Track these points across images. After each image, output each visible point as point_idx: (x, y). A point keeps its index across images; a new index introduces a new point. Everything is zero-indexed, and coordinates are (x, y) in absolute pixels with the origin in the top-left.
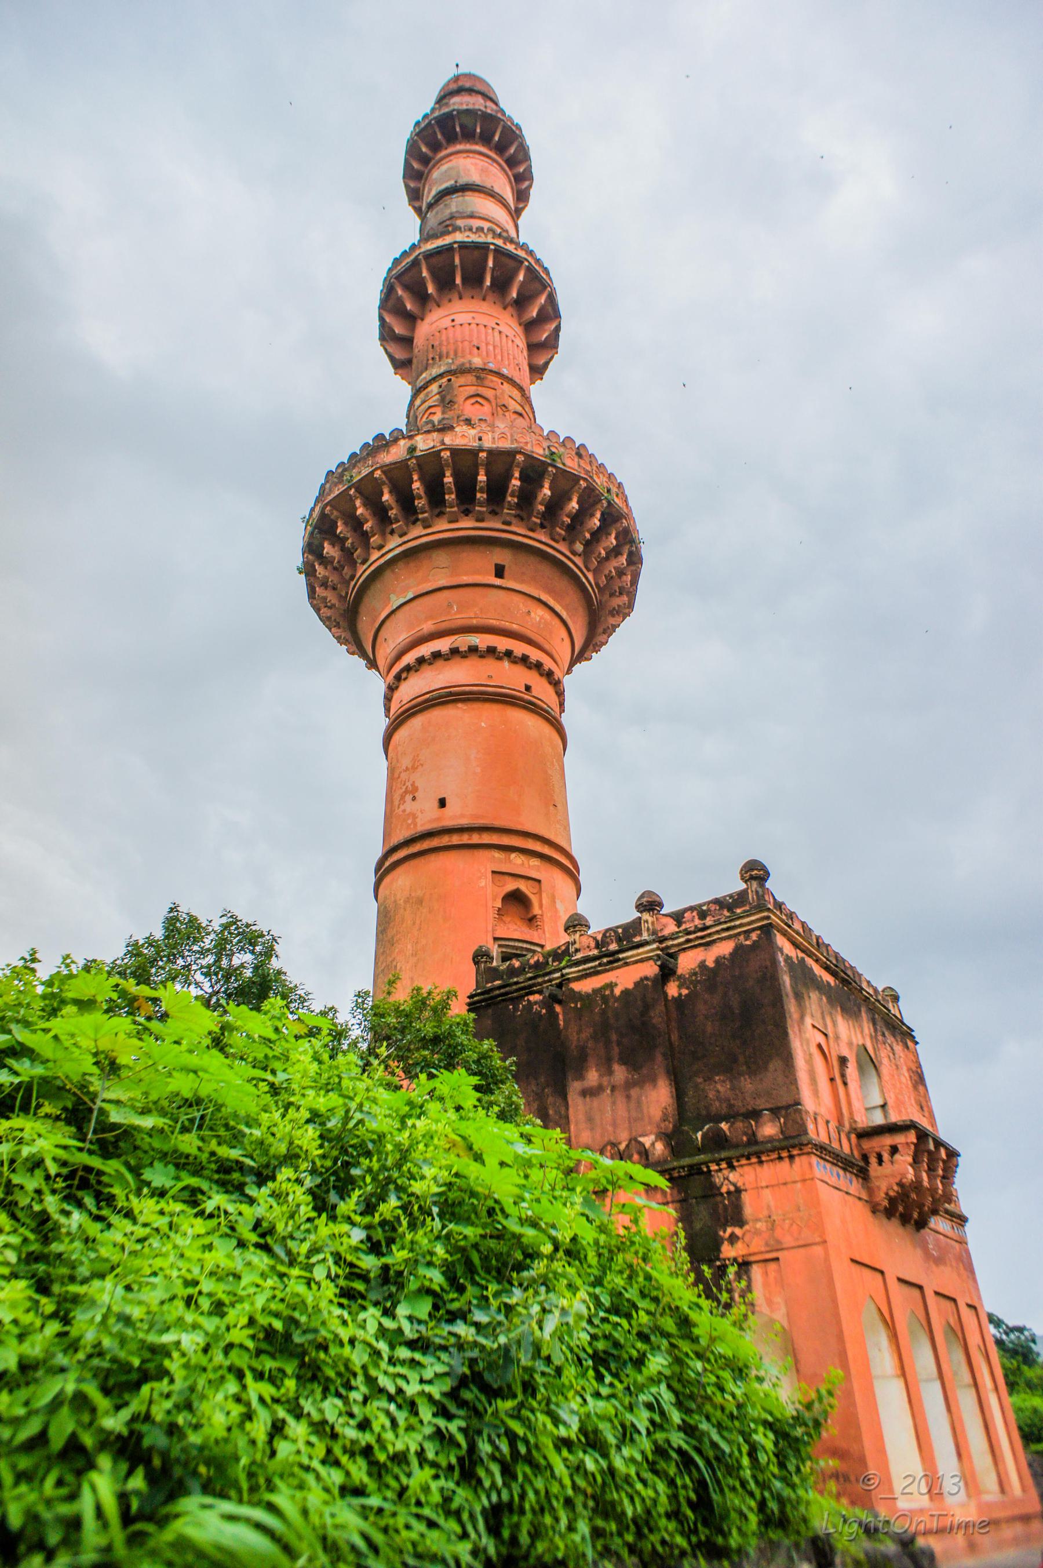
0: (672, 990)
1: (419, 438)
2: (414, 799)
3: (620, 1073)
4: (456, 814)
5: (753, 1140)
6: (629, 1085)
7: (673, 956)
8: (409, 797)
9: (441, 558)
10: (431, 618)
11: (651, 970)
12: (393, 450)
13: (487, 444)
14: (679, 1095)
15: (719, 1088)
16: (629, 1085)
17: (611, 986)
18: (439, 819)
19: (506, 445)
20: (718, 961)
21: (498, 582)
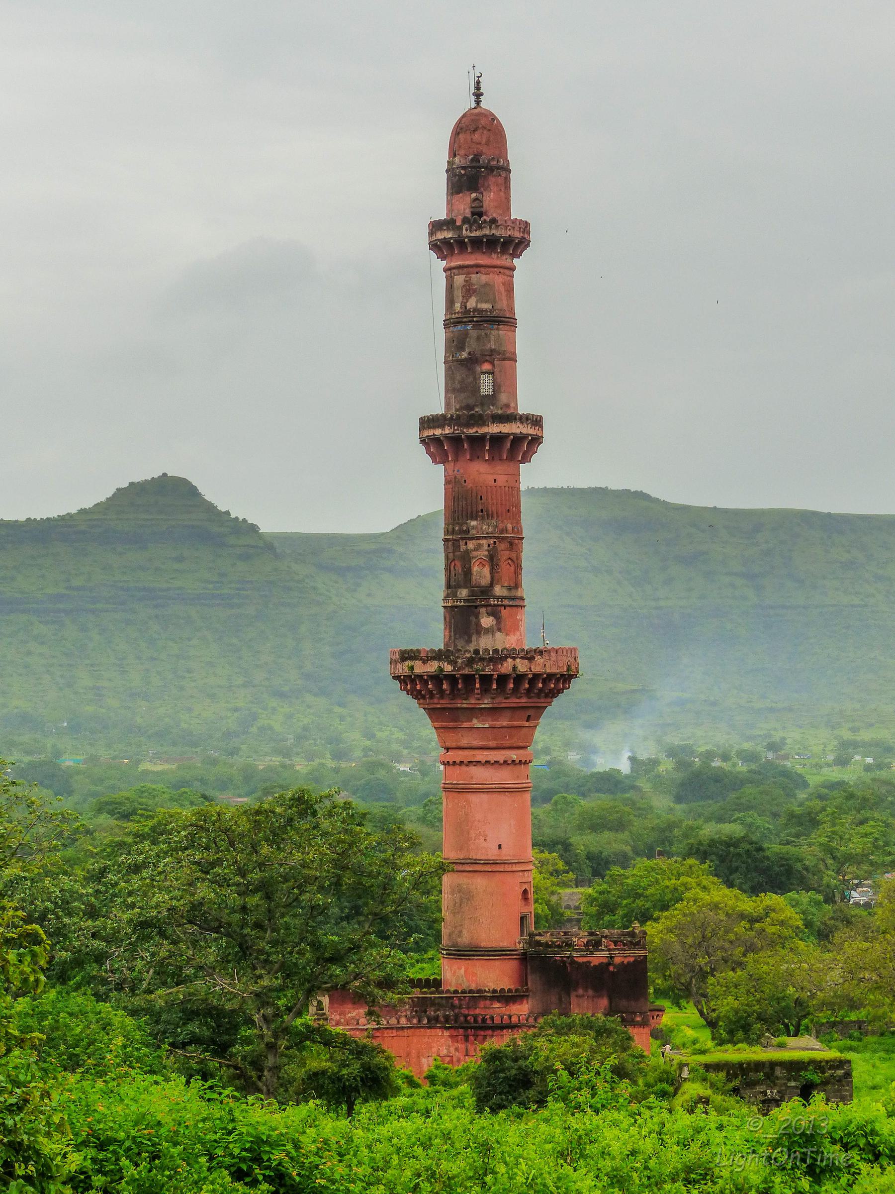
0: (611, 969)
1: (518, 660)
2: (485, 840)
3: (590, 992)
4: (507, 854)
5: (633, 1020)
6: (593, 997)
7: (612, 957)
8: (482, 838)
9: (508, 713)
10: (495, 739)
11: (605, 961)
12: (505, 665)
13: (548, 671)
14: (611, 1002)
15: (624, 1003)
16: (593, 997)
17: (590, 962)
18: (499, 855)
19: (554, 670)
20: (628, 963)
21: (527, 724)
